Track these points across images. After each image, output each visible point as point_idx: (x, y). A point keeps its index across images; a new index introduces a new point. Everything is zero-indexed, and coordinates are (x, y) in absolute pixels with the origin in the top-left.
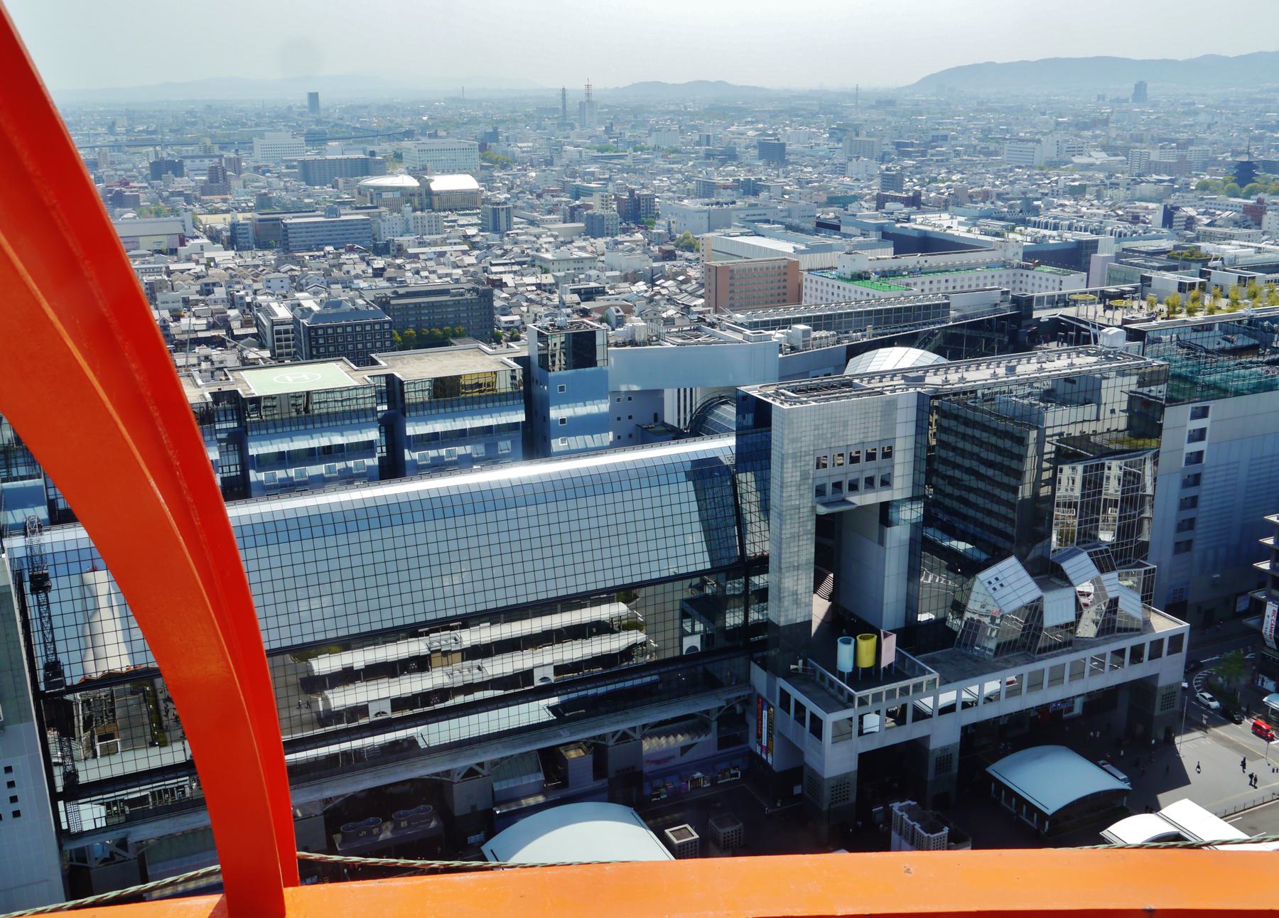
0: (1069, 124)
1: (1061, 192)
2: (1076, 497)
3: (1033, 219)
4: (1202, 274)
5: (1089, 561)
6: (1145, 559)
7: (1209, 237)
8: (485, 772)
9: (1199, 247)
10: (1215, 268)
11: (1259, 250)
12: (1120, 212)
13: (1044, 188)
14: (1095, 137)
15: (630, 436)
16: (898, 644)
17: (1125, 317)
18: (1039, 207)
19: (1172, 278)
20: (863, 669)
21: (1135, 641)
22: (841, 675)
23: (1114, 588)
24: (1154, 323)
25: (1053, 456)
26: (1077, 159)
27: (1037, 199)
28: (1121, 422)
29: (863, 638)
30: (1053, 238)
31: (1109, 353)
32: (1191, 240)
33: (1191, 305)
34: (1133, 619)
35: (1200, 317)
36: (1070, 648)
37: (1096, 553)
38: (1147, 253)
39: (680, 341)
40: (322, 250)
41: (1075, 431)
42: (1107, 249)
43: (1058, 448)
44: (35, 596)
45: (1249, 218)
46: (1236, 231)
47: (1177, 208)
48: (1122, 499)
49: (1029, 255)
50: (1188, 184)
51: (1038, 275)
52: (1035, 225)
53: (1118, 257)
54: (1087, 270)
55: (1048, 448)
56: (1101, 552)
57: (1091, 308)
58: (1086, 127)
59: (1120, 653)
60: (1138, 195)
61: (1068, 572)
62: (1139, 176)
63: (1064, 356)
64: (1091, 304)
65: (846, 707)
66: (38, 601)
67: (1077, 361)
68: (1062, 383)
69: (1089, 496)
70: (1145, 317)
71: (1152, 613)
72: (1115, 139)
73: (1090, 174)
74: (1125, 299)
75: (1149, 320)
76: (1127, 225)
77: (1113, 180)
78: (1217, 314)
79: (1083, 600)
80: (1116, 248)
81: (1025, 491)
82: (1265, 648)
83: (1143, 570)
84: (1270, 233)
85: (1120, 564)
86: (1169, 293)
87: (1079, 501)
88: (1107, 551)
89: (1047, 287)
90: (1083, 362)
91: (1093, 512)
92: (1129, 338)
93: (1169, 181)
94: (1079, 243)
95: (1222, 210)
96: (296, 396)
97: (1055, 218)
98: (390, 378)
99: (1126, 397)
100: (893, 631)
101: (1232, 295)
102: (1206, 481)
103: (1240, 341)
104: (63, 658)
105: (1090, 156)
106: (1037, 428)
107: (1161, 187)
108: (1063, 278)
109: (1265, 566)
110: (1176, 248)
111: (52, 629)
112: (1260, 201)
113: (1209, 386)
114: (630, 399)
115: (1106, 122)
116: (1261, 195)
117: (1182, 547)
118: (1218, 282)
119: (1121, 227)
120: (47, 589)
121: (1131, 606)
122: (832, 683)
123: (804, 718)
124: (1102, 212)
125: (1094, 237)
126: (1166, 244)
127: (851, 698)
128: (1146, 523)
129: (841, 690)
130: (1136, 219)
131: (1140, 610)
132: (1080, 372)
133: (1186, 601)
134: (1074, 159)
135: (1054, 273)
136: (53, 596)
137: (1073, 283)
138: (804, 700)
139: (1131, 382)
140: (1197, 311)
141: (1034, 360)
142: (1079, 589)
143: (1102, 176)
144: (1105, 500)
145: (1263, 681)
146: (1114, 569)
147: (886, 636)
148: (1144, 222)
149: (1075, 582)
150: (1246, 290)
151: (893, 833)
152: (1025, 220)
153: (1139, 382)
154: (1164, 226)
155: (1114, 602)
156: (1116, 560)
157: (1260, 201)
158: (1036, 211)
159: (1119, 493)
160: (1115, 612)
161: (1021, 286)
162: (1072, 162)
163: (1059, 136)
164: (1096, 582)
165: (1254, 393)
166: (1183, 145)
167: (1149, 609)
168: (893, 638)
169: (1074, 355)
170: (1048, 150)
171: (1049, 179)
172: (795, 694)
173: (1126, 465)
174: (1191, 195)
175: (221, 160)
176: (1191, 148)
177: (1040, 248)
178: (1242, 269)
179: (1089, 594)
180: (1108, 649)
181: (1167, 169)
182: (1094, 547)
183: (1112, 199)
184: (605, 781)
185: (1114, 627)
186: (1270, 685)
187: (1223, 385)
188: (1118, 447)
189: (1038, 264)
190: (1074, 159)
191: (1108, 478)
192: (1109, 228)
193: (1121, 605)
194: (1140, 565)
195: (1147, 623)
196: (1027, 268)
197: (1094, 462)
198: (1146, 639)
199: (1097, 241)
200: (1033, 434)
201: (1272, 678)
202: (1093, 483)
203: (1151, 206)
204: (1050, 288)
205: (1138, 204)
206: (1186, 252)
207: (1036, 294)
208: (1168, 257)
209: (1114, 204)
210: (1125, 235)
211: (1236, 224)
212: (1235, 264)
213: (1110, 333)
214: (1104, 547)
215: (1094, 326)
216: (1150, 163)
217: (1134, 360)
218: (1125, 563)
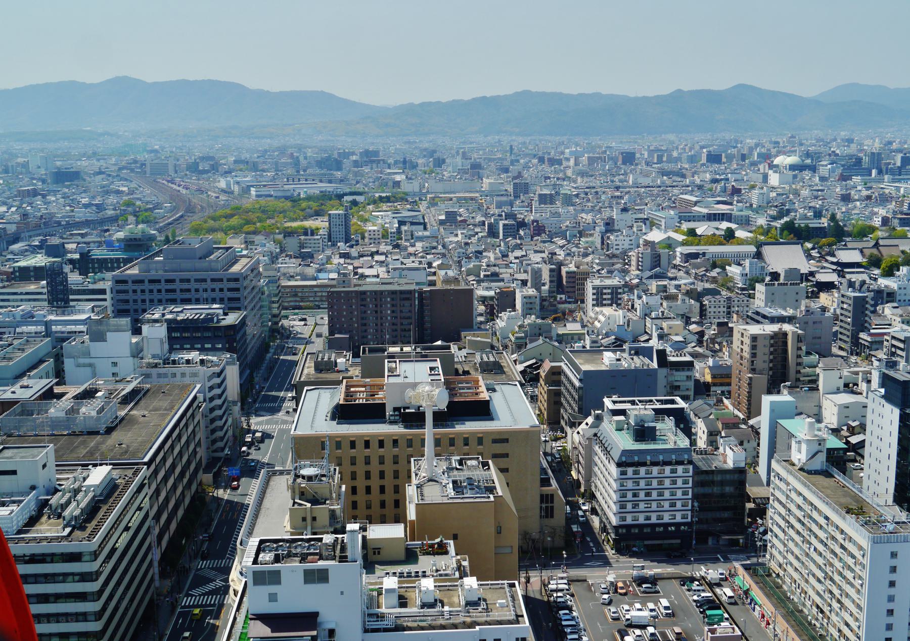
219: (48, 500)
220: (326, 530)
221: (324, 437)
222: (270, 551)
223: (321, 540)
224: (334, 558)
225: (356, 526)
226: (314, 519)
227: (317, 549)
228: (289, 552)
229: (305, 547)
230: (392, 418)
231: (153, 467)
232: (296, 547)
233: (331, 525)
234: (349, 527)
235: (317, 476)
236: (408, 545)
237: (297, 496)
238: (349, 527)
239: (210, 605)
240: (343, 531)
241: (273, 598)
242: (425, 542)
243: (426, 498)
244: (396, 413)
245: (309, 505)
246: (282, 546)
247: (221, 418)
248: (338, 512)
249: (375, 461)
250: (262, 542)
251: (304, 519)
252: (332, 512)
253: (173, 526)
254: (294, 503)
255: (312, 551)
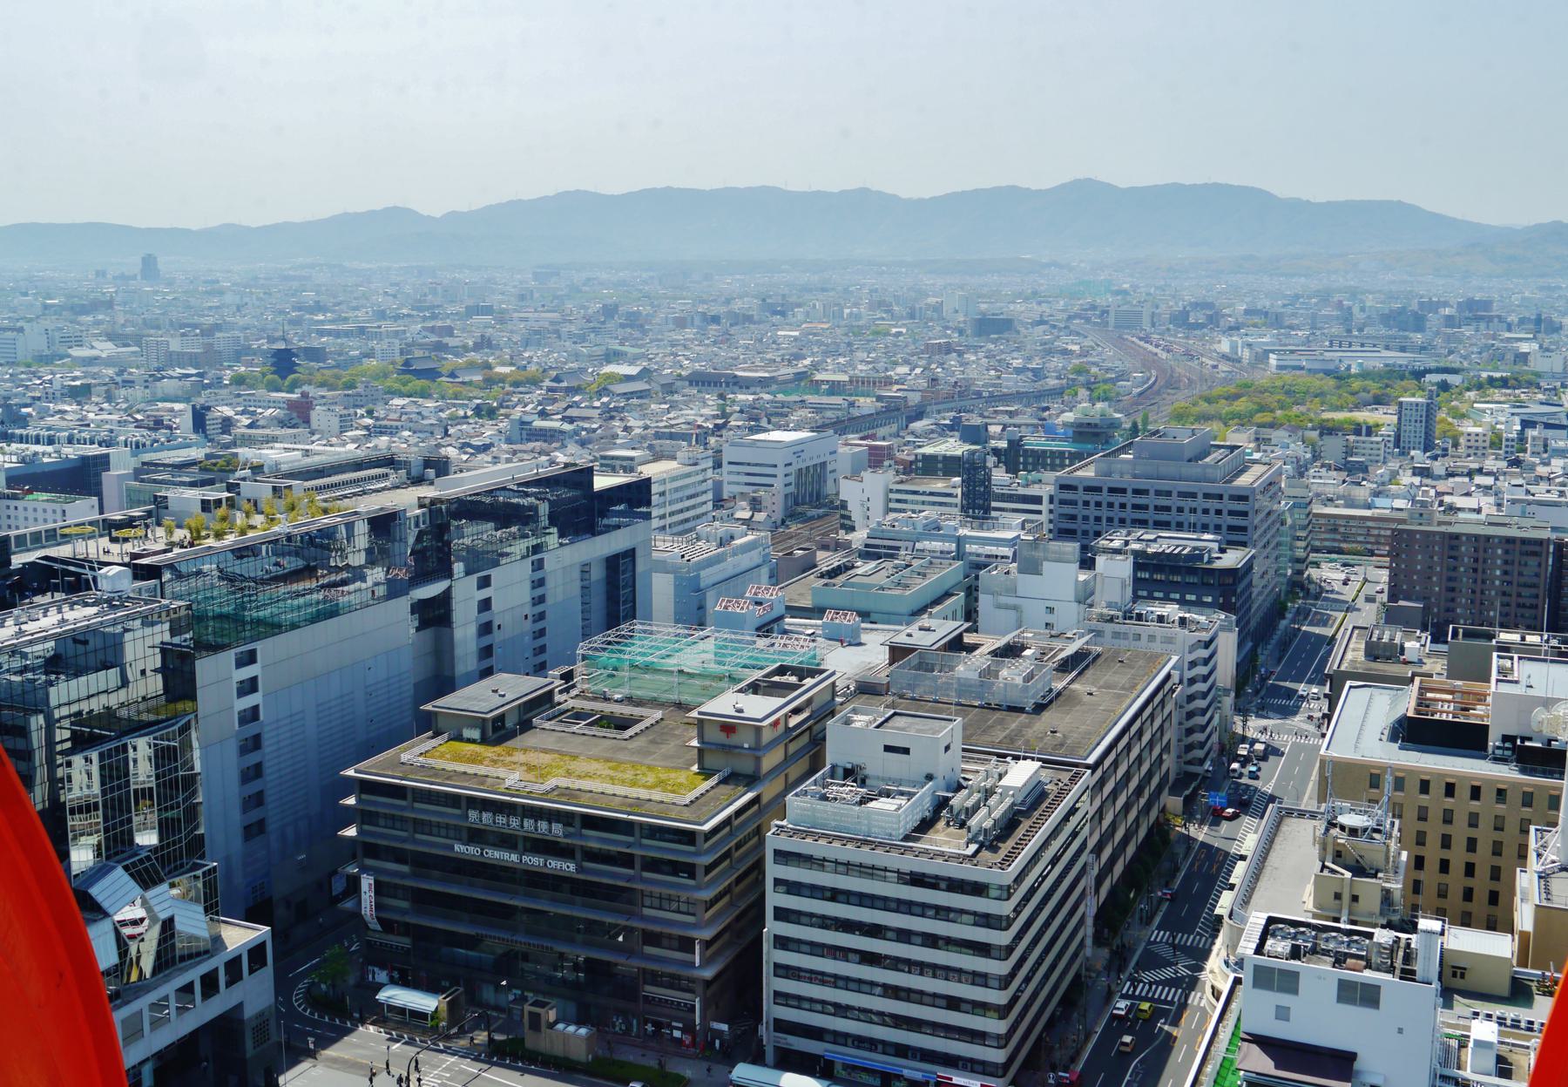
0: (62, 307)
1: (58, 394)
2: (95, 796)
3: (18, 432)
4: (230, 488)
5: (126, 877)
6: (202, 857)
7: (248, 441)
9: (236, 455)
10: (244, 479)
11: (307, 453)
12: (139, 417)
13: (34, 390)
14: (98, 323)
17: (136, 550)
18: (30, 415)
19: (195, 494)
21: (204, 968)
23: (166, 905)
24: (170, 555)
25: (68, 745)
26: (76, 352)
27: (26, 406)
28: (155, 684)
30: (47, 455)
31: (113, 599)
32: (226, 446)
33: (218, 526)
34: (197, 939)
35: (230, 539)
36: (118, 1002)
37: (134, 864)
38: (173, 466)
41: (96, 705)
42: (122, 464)
43: (74, 732)
45: (295, 415)
46: (278, 432)
47: (208, 408)
48: (158, 786)
49: (13, 480)
50: (220, 378)
51: (30, 506)
52: (21, 439)
53: (137, 474)
54: (99, 494)
55: (62, 734)
56: (141, 861)
57: (91, 543)
58: (84, 310)
59: (188, 989)
60: (160, 394)
61: (99, 899)
62: (158, 370)
63: (53, 611)
64: (89, 538)
67: (70, 615)
68: (70, 642)
69: (112, 789)
70: (163, 547)
71: (223, 925)
72: (123, 325)
73: (95, 369)
74: (136, 527)
75: (165, 551)
76: (145, 432)
77: (126, 376)
78: (251, 534)
79: (127, 931)
80: (134, 463)
81: (39, 797)
82: (370, 933)
83: (199, 873)
84: (321, 432)
85: (170, 872)
86: (190, 515)
87: (100, 800)
88: (148, 858)
89: (36, 520)
90: (80, 615)
91: (121, 811)
92: (136, 577)
93: (197, 375)
94: (84, 459)
95: (264, 408)
97: (49, 429)
99: (158, 650)
101: (267, 509)
102: (267, 741)
103: (290, 563)
105: (93, 347)
106: (41, 712)
107: (187, 383)
108: (66, 507)
109: (351, 832)
110: (208, 456)
112: (304, 395)
113: (259, 622)
115: (110, 304)
116: (306, 388)
117: (253, 831)
118: (249, 496)
119: (139, 435)
121: (193, 923)
124: (115, 417)
125: (104, 450)
126: (196, 453)
128: (202, 809)
130: (158, 424)
131: (204, 926)
132: (74, 630)
133: (271, 897)
134: (70, 351)
135: (53, 501)
137: (83, 509)
139: (161, 633)
140: (226, 534)
141: (10, 622)
142: (117, 918)
143: (110, 372)
144: (136, 791)
145: (374, 973)
146: (161, 881)
148: (170, 428)
149: (110, 911)
150: (282, 503)
152: (6, 433)
153: (171, 630)
154: (196, 430)
155: (168, 925)
156: (163, 868)
157: (304, 395)
158: (23, 421)
159: (153, 779)
160: (173, 936)
161: (9, 522)
162: (69, 356)
163: (47, 323)
164: (145, 903)
165: (312, 623)
166: (209, 331)
167: (218, 921)
169: (66, 608)
170: (33, 340)
171: (39, 378)
173: (155, 739)
174: (224, 392)
176: (218, 335)
177: (31, 470)
178: (276, 477)
179: (142, 920)
180: (170, 988)
181: (193, 360)
182: (129, 858)
183: (126, 400)
185: (174, 957)
186: (382, 976)
187: (276, 619)
188: (152, 717)
189: (30, 492)
190: (70, 351)
191: (135, 761)
192: (122, 438)
193: (178, 926)
194: (196, 867)
195: (217, 941)
196: (15, 497)
197: (112, 745)
198: (217, 962)
199: (107, 456)
200: (38, 721)
201: (382, 967)
202: (115, 772)
203: (178, 406)
204: (40, 520)
205: (160, 405)
206: (221, 462)
207: (13, 533)
208: (201, 469)
209: (130, 407)
210: (144, 445)
211: (282, 423)
212: (278, 470)
213: (110, 574)
214: (144, 854)
215: (92, 569)
216: (171, 354)
217: (146, 604)
218: (176, 868)
219: (947, 799)
220: (1373, 920)
221: (1384, 768)
222: (1284, 938)
223: (1370, 936)
224: (1391, 969)
225: (1436, 925)
226: (1355, 898)
227: (1362, 950)
228: (1315, 945)
229: (1343, 942)
230: (1499, 752)
231: (1099, 773)
232: (1327, 940)
233: (1382, 914)
234: (1424, 924)
235: (1365, 830)
236: (1516, 972)
237: (1329, 857)
238: (1424, 924)
239: (1165, 1002)
240: (1412, 927)
241: (1282, 1014)
242: (1548, 974)
243: (1554, 898)
244: (1507, 745)
245: (1348, 875)
246: (1303, 933)
247: (1204, 712)
248: (1397, 896)
249: (1461, 820)
250: (1271, 921)
251: (1338, 896)
252: (1387, 896)
253: (1119, 868)
254: (1324, 867)
255: (1353, 951)
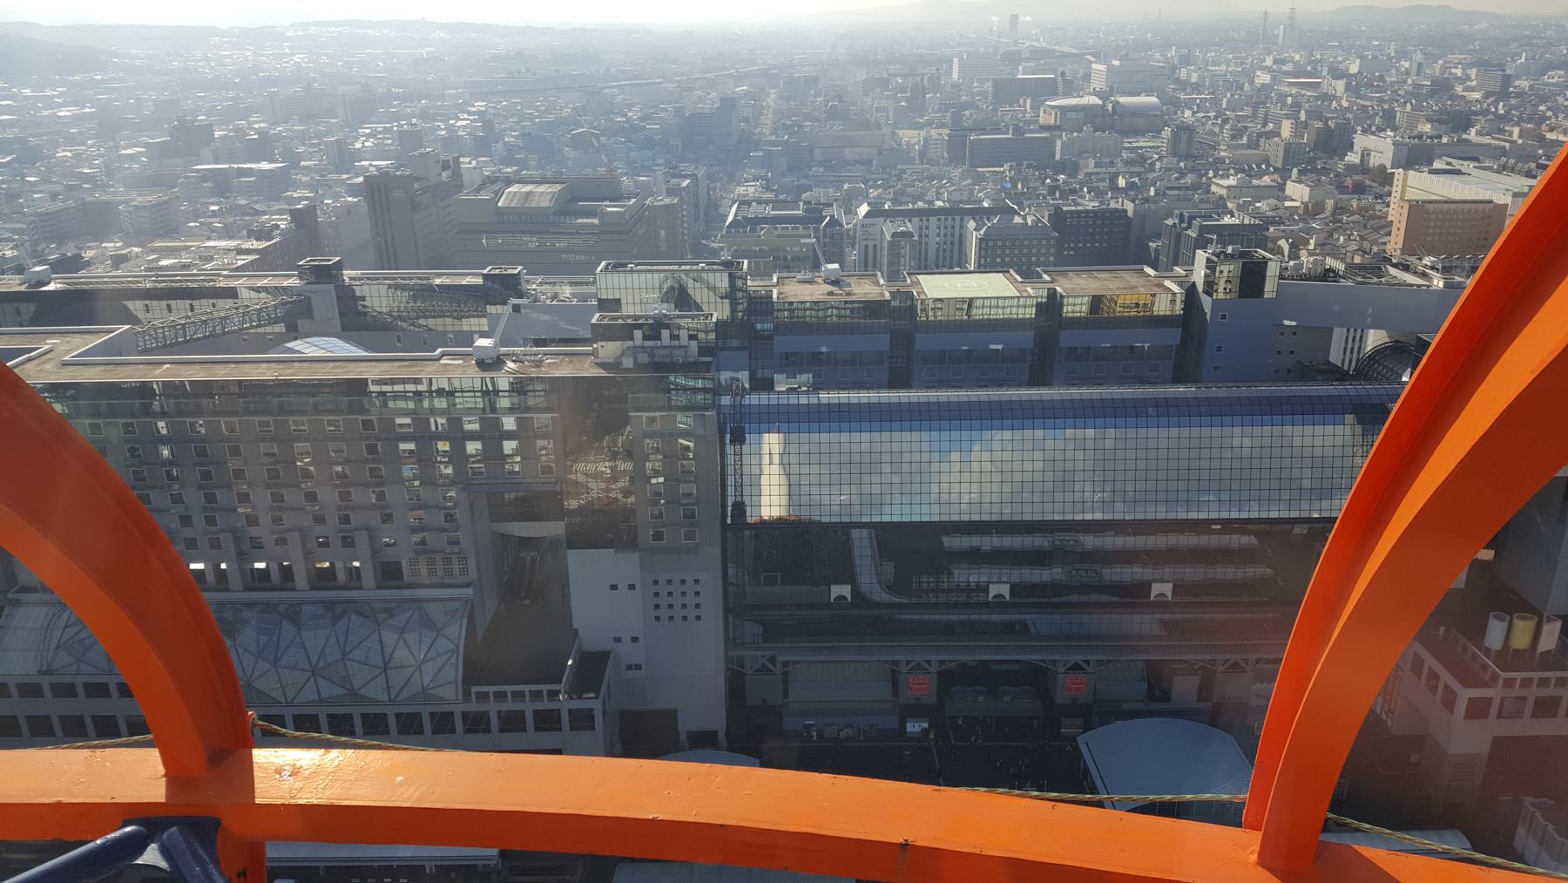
8: (1090, 669)
15: (1289, 371)
16: (1563, 631)
20: (1515, 650)
22: (1487, 652)
29: (1522, 618)
39: (1360, 279)
40: (1003, 167)
44: (732, 447)
65: (1486, 685)
66: (735, 451)
96: (963, 301)
98: (1052, 294)
100: (1559, 617)
104: (747, 500)
111: (742, 475)
114: (1294, 334)
120: (742, 441)
122: (1475, 657)
123: (1436, 687)
127: (1495, 677)
129: (1484, 667)
136: (745, 448)
138: (1439, 669)
147: (1549, 620)
151: (1520, 827)
168: (1559, 624)
172: (1431, 662)
175: (922, 80)
184: (1210, 704)
